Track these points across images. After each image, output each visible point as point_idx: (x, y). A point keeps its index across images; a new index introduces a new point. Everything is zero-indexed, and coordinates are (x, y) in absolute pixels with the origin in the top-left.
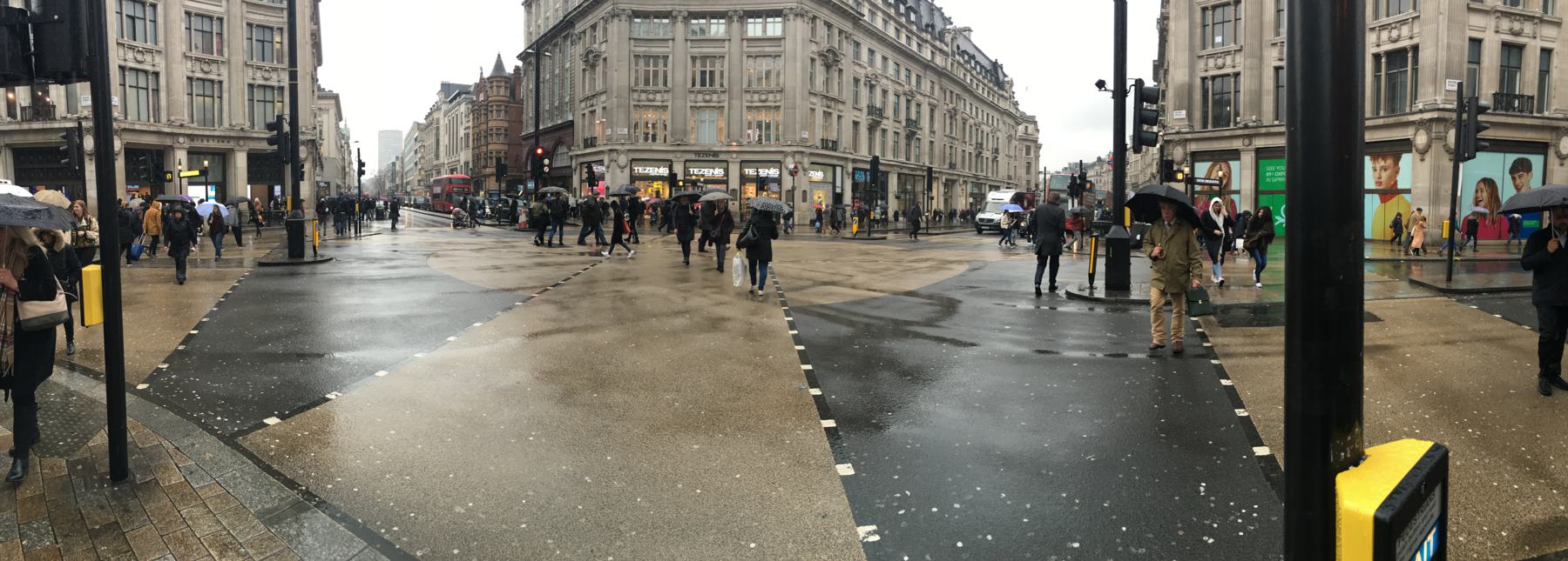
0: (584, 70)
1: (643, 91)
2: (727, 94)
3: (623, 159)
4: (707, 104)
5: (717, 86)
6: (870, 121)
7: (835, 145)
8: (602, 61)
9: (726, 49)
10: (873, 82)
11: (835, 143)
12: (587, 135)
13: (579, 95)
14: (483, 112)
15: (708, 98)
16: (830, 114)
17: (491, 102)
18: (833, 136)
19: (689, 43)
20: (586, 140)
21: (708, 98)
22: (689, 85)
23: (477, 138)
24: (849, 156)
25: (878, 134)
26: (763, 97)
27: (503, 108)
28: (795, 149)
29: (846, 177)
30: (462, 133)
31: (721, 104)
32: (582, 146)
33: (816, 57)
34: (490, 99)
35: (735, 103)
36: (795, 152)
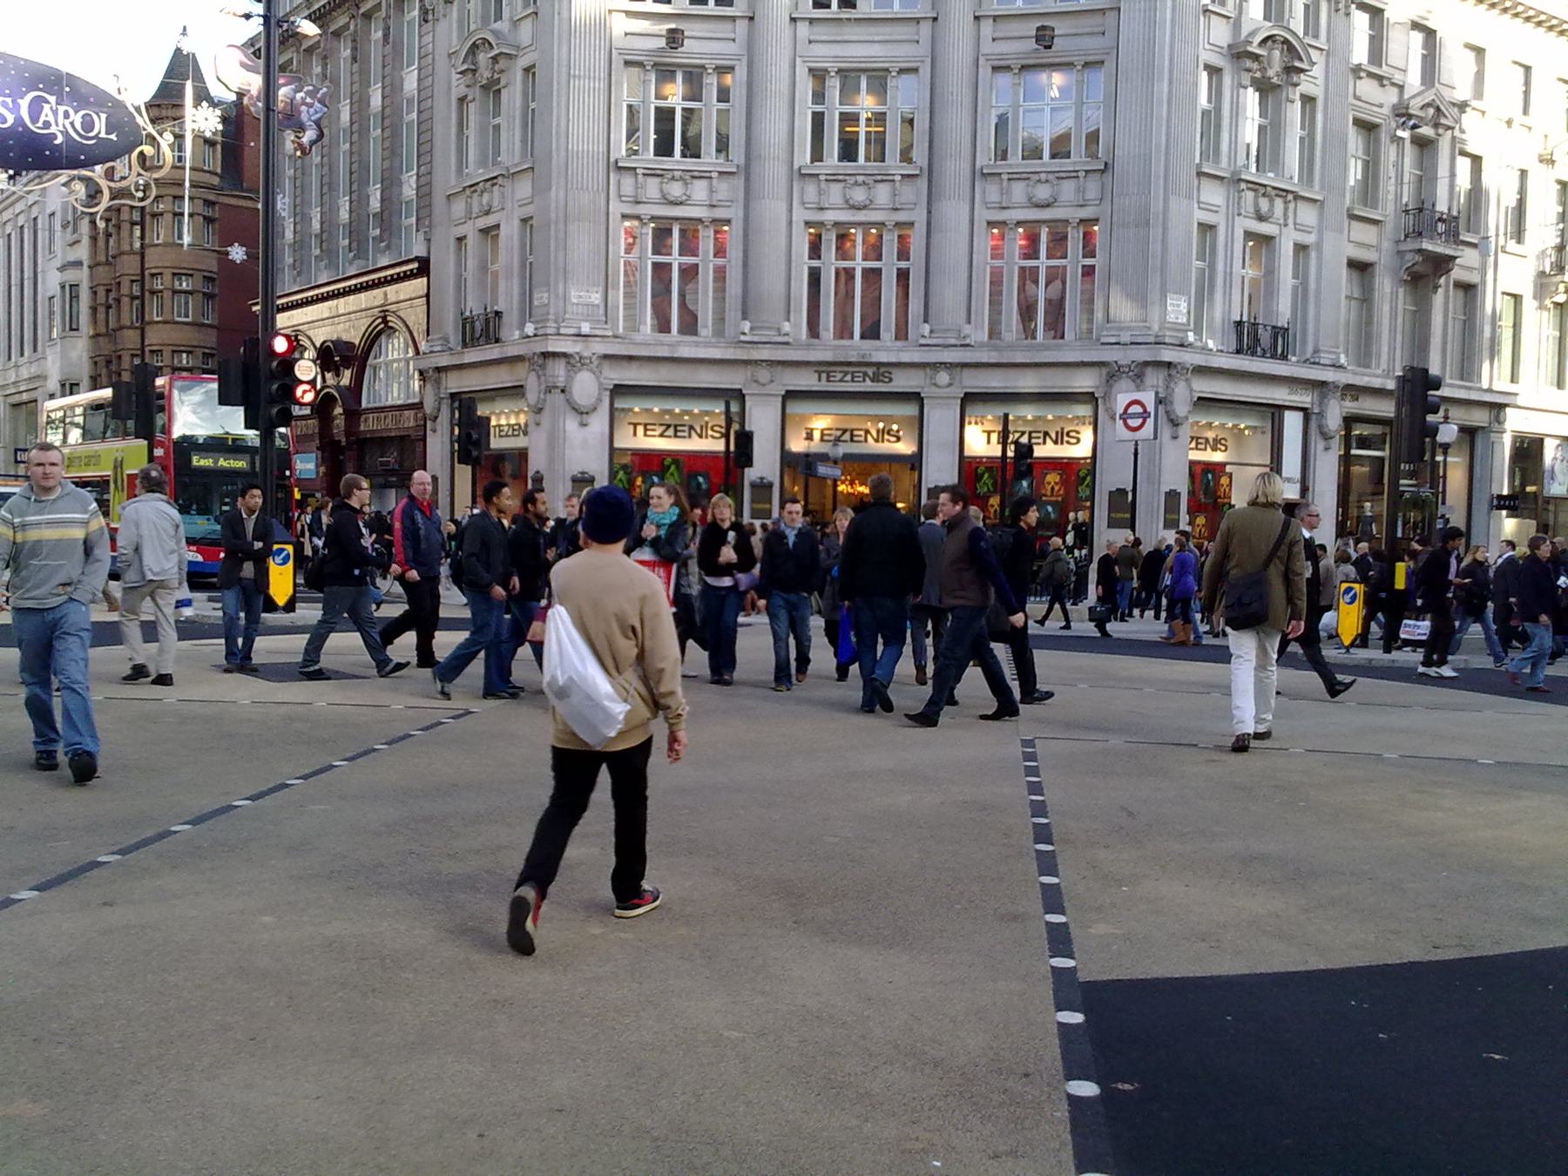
0: (462, 100)
1: (652, 173)
2: (923, 184)
3: (585, 386)
4: (861, 216)
5: (893, 162)
6: (1411, 259)
7: (1279, 342)
8: (519, 75)
9: (923, 49)
10: (1426, 131)
11: (1283, 332)
12: (473, 306)
13: (446, 178)
15: (859, 195)
16: (1268, 240)
18: (1283, 311)
19: (803, 29)
20: (466, 323)
21: (859, 195)
22: (804, 156)
23: (107, 299)
24: (1329, 376)
25: (1442, 302)
26: (1043, 193)
28: (1143, 355)
29: (1317, 444)
30: (52, 282)
31: (902, 217)
32: (454, 339)
33: (1217, 61)
35: (954, 213)
36: (1146, 364)
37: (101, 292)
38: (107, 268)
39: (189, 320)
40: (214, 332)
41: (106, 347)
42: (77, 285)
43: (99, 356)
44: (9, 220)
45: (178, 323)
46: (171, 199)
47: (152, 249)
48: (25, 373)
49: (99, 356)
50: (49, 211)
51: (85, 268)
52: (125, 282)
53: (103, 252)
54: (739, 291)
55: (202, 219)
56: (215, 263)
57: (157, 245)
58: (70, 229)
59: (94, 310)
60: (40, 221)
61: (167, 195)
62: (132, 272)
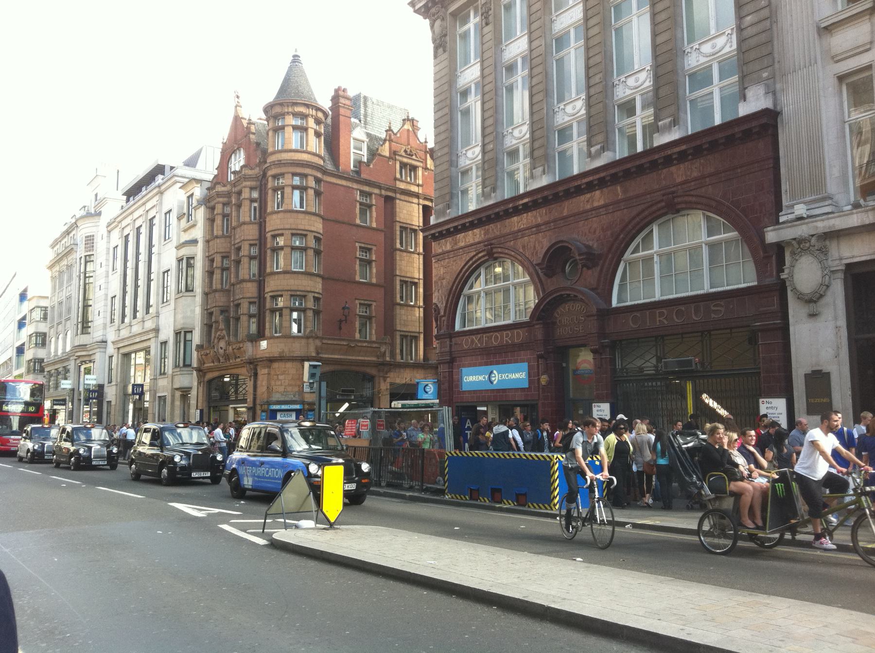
14: (246, 194)
17: (280, 164)
27: (312, 183)
34: (271, 159)
37: (218, 259)
38: (222, 240)
40: (319, 280)
41: (220, 300)
42: (193, 258)
43: (215, 307)
44: (129, 224)
45: (295, 273)
46: (290, 175)
47: (274, 216)
48: (136, 329)
49: (215, 307)
50: (165, 210)
51: (200, 245)
53: (220, 228)
54: (814, 214)
55: (313, 191)
56: (321, 226)
57: (279, 212)
58: (184, 220)
59: (210, 273)
60: (155, 221)
61: (288, 173)
62: (251, 238)
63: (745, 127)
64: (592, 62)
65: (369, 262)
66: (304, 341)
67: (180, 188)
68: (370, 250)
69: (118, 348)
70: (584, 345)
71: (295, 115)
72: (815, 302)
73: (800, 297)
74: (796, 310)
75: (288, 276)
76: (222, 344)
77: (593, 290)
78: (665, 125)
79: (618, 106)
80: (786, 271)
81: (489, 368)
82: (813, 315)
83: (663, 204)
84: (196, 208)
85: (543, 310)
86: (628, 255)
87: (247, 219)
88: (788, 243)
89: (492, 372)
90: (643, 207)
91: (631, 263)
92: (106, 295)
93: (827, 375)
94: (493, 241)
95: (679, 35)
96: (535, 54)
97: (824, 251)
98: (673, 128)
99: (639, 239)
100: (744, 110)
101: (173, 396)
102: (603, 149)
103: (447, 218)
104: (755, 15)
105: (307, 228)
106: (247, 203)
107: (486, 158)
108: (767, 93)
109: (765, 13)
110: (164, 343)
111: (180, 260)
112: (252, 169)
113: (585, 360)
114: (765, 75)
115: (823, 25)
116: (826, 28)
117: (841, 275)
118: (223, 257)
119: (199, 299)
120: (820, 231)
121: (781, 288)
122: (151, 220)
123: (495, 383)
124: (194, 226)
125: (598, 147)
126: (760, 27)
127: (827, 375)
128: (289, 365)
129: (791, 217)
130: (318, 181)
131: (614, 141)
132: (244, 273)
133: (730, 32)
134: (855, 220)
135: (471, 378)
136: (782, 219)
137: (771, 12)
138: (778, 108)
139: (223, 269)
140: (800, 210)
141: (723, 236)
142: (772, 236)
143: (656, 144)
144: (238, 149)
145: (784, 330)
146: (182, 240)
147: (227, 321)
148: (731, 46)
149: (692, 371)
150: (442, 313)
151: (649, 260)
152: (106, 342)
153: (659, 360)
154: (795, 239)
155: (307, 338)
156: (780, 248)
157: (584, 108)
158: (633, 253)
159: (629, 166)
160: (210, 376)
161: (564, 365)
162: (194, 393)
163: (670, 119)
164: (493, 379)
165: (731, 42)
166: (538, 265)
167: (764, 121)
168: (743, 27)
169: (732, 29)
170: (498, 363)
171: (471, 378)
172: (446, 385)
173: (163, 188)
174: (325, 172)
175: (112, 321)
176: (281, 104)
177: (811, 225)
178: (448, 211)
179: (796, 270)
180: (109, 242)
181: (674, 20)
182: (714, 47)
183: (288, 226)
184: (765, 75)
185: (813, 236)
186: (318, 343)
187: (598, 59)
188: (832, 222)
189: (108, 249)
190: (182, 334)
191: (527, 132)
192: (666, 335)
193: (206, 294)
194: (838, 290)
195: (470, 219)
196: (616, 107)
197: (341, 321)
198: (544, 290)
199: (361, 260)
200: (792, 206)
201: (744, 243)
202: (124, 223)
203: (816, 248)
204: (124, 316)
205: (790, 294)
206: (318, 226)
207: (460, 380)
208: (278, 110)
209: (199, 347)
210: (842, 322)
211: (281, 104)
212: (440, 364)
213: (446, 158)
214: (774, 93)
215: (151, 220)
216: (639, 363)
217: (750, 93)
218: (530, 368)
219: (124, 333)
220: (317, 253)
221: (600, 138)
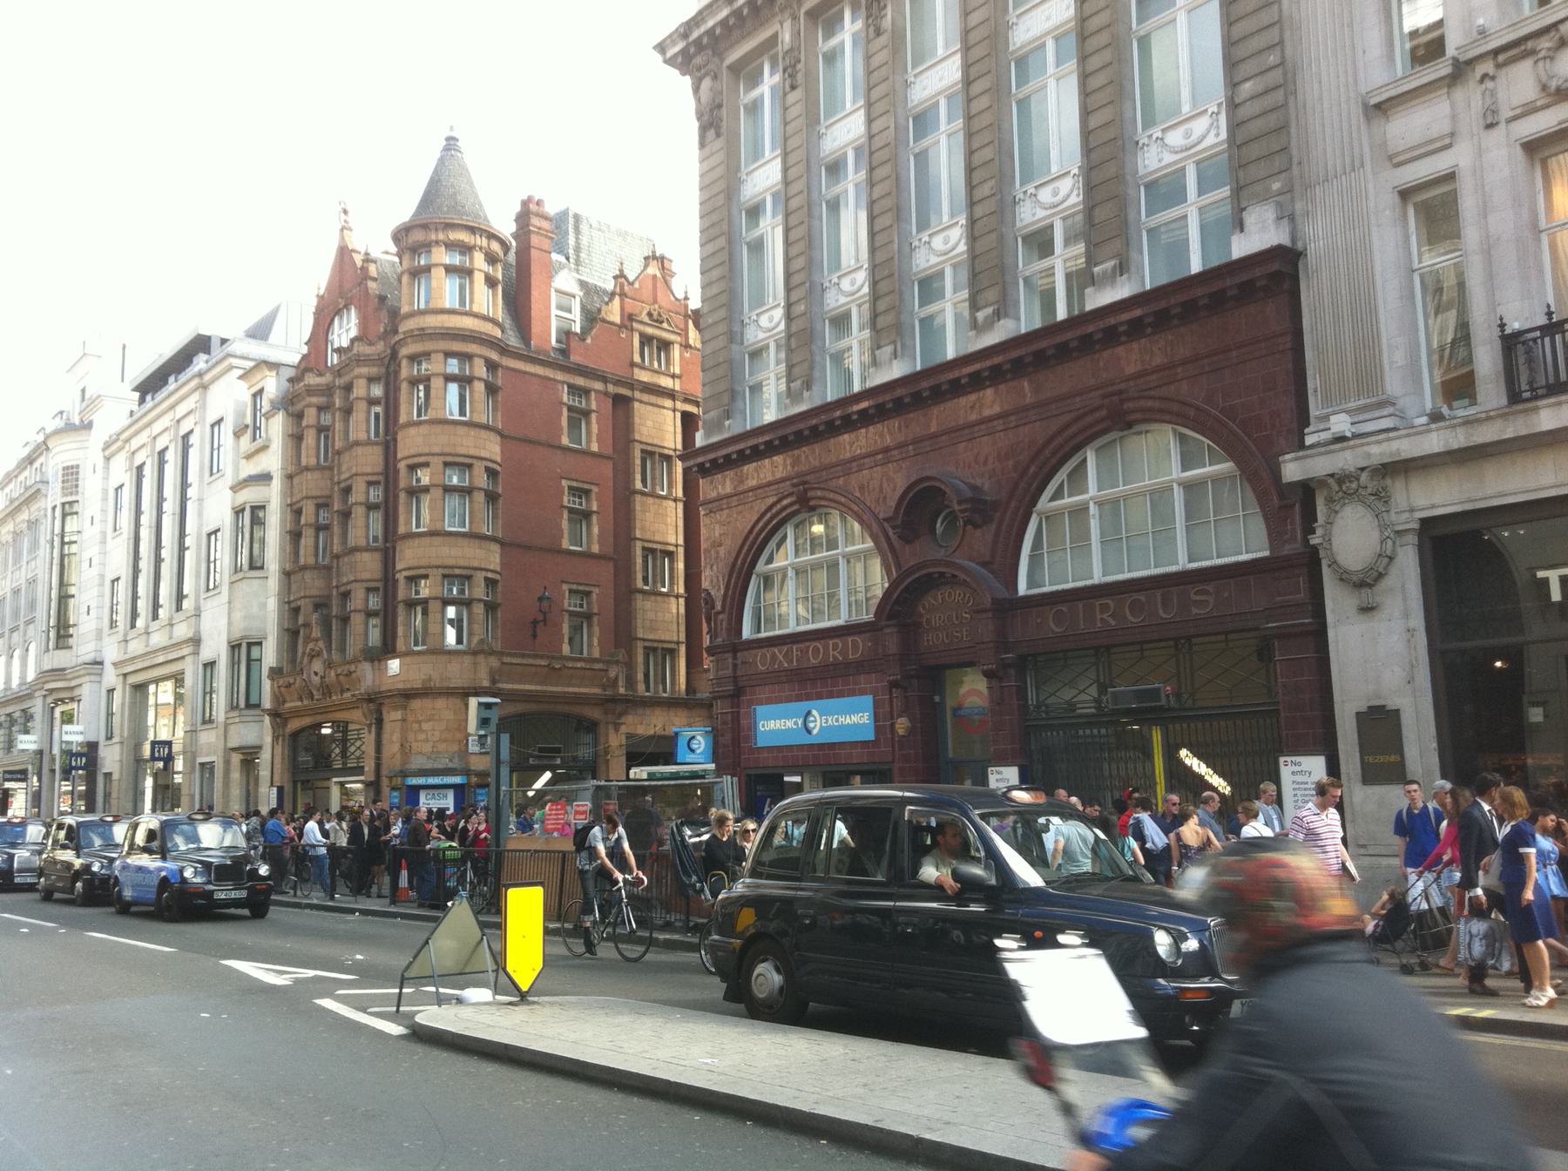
14: (359, 390)
17: (423, 334)
27: (481, 370)
37: (309, 509)
38: (317, 475)
39: (466, 530)
40: (496, 548)
41: (313, 584)
42: (263, 507)
43: (305, 597)
44: (143, 446)
45: (451, 534)
46: (441, 357)
47: (412, 431)
48: (158, 639)
49: (305, 597)
50: (211, 418)
51: (277, 482)
52: (359, 488)
53: (313, 452)
57: (420, 423)
58: (246, 439)
59: (294, 536)
60: (193, 440)
61: (437, 351)
62: (369, 470)
63: (1244, 277)
64: (978, 159)
65: (587, 515)
66: (468, 659)
67: (240, 378)
68: (587, 492)
69: (125, 675)
70: (971, 664)
71: (450, 246)
72: (1370, 586)
73: (1344, 577)
74: (1337, 601)
75: (437, 540)
76: (317, 666)
77: (984, 564)
78: (1105, 272)
79: (1024, 239)
80: (1319, 532)
81: (803, 706)
82: (1367, 610)
83: (1104, 412)
84: (268, 416)
85: (897, 602)
86: (1044, 503)
87: (362, 436)
88: (1321, 482)
89: (809, 713)
90: (1067, 418)
91: (1049, 517)
92: (102, 576)
93: (1396, 713)
94: (808, 478)
95: (1128, 115)
96: (878, 143)
97: (1382, 496)
98: (1118, 278)
99: (1061, 475)
100: (1241, 247)
101: (227, 762)
102: (998, 315)
103: (726, 435)
104: (1258, 79)
105: (472, 452)
106: (362, 405)
107: (794, 329)
108: (1279, 218)
109: (1275, 77)
110: (210, 665)
111: (238, 512)
112: (371, 344)
113: (972, 690)
114: (1276, 186)
115: (1374, 101)
116: (1378, 106)
117: (1412, 539)
118: (318, 506)
119: (273, 583)
120: (1375, 461)
121: (1311, 562)
122: (186, 437)
123: (815, 732)
124: (264, 448)
125: (990, 310)
126: (1268, 101)
127: (1396, 713)
128: (441, 703)
129: (1324, 436)
130: (492, 366)
131: (1018, 302)
132: (356, 535)
133: (1215, 109)
134: (1434, 442)
135: (773, 725)
136: (1309, 440)
137: (1285, 74)
138: (1300, 246)
139: (319, 528)
140: (1340, 424)
141: (1208, 469)
142: (1293, 470)
143: (1089, 307)
144: (346, 306)
145: (1318, 634)
146: (243, 475)
147: (326, 625)
148: (1217, 135)
149: (1161, 708)
150: (718, 607)
151: (1080, 511)
152: (101, 663)
153: (1102, 689)
154: (1332, 475)
155: (475, 653)
156: (1307, 490)
157: (963, 241)
158: (1053, 499)
159: (1043, 344)
160: (294, 725)
161: (937, 699)
162: (265, 756)
163: (1113, 263)
164: (812, 725)
165: (1218, 127)
166: (885, 520)
167: (1276, 267)
168: (1237, 101)
169: (1219, 105)
170: (820, 697)
171: (773, 725)
172: (728, 737)
173: (207, 378)
174: (504, 350)
175: (113, 624)
176: (425, 227)
177: (1360, 451)
178: (727, 423)
179: (1336, 530)
180: (106, 478)
181: (1118, 89)
182: (1188, 135)
183: (436, 450)
184: (1276, 186)
185: (1362, 469)
186: (494, 662)
187: (987, 153)
188: (1395, 445)
189: (105, 491)
190: (243, 649)
191: (864, 283)
192: (1115, 646)
193: (287, 575)
194: (1408, 567)
195: (767, 438)
196: (1020, 240)
197: (535, 623)
198: (898, 566)
199: (571, 511)
200: (1326, 418)
201: (1246, 484)
202: (135, 443)
203: (1369, 490)
204: (134, 615)
205: (1326, 572)
206: (492, 448)
207: (753, 727)
208: (418, 236)
209: (275, 673)
210: (1418, 621)
211: (425, 227)
212: (715, 698)
213: (722, 328)
214: (1292, 218)
215: (186, 437)
216: (1067, 694)
217: (1250, 218)
218: (877, 705)
219: (136, 647)
220: (492, 497)
221: (991, 295)
